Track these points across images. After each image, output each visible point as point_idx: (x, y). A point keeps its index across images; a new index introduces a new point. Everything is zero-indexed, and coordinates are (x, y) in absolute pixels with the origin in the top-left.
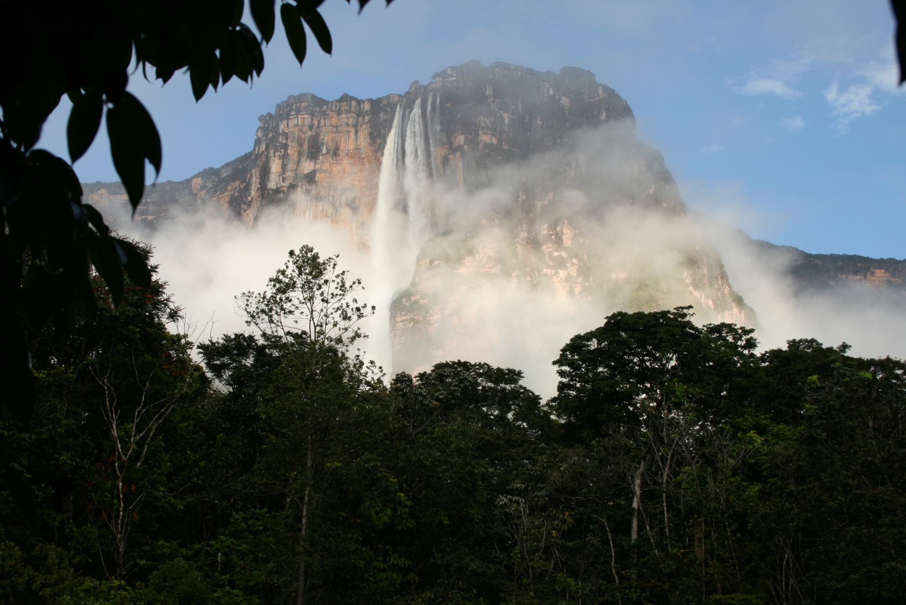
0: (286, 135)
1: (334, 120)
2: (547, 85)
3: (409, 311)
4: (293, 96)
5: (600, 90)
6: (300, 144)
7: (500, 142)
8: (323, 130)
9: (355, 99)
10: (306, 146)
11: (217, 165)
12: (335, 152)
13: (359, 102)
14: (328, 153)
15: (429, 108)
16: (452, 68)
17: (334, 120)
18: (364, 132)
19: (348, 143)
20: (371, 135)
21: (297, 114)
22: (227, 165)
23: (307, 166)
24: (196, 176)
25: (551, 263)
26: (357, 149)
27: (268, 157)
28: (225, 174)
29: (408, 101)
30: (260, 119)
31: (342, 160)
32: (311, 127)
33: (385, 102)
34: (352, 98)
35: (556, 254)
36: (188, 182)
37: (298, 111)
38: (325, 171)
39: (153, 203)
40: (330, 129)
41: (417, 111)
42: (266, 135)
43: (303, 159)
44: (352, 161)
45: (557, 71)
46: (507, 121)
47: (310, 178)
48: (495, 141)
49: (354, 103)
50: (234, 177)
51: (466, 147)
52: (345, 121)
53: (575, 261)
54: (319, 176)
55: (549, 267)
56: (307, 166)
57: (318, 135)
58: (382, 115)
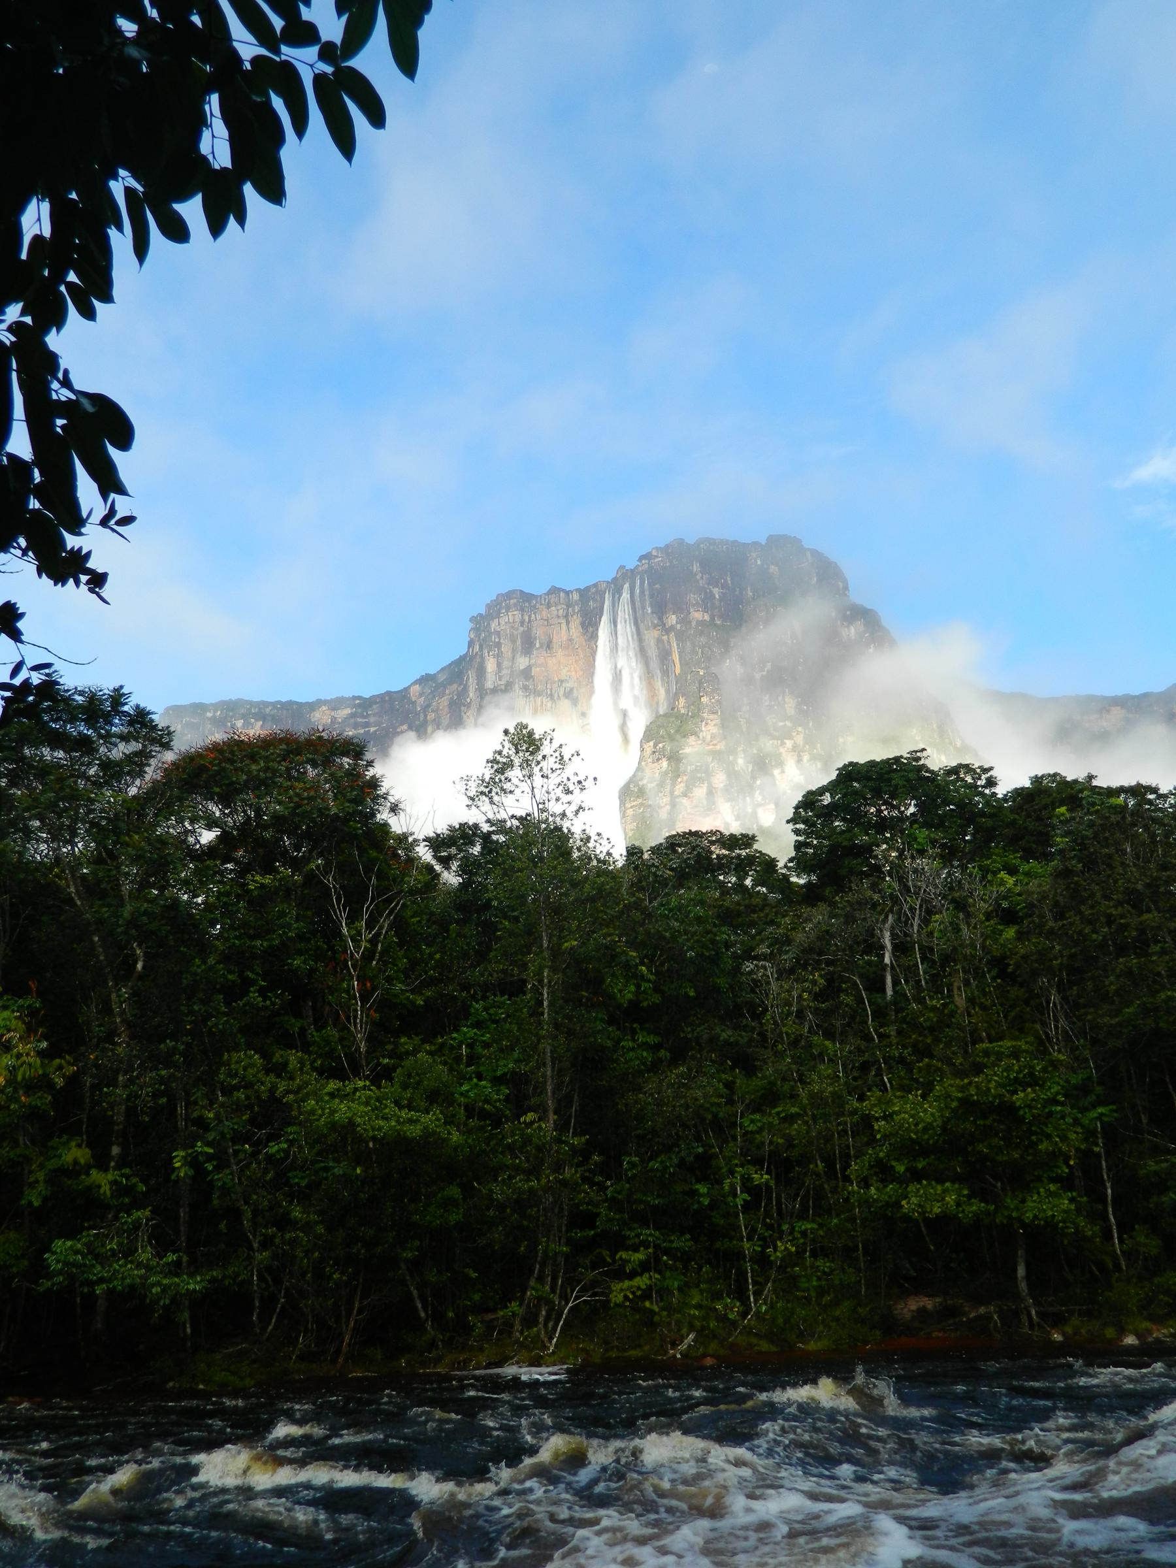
0: (498, 634)
1: (545, 614)
2: (754, 555)
4: (502, 595)
5: (808, 554)
6: (514, 641)
7: (712, 618)
8: (535, 624)
9: (563, 590)
10: (519, 642)
11: (432, 671)
12: (549, 646)
13: (567, 593)
14: (541, 646)
15: (637, 591)
16: (657, 548)
17: (545, 614)
18: (576, 622)
19: (561, 635)
20: (583, 624)
21: (507, 612)
22: (443, 669)
24: (415, 683)
25: (776, 734)
26: (571, 640)
27: (482, 657)
28: (442, 678)
29: (615, 587)
30: (472, 619)
32: (522, 623)
33: (593, 590)
34: (560, 590)
35: (781, 724)
36: (406, 689)
37: (508, 609)
39: (374, 715)
41: (626, 595)
42: (478, 636)
43: (518, 656)
45: (763, 542)
47: (527, 673)
48: (707, 617)
49: (562, 594)
50: (450, 681)
51: (678, 626)
53: (800, 729)
54: (535, 671)
56: (522, 662)
57: (529, 630)
58: (591, 603)
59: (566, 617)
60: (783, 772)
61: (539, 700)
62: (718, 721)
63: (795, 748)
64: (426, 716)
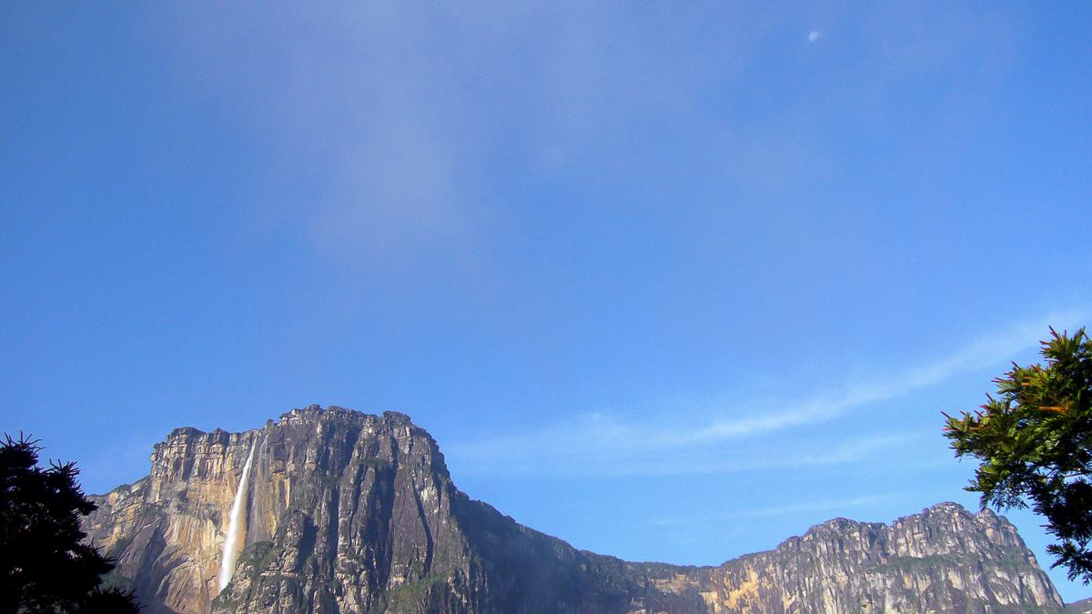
0: (168, 460)
3: (223, 607)
5: (407, 429)
6: (177, 466)
13: (228, 435)
22: (137, 482)
23: (181, 486)
28: (135, 489)
31: (210, 480)
35: (347, 561)
37: (180, 440)
38: (195, 490)
40: (203, 455)
44: (218, 482)
45: (380, 415)
46: (332, 453)
47: (183, 496)
50: (139, 493)
52: (216, 450)
55: (342, 572)
59: (223, 453)
60: (342, 600)
61: (187, 517)
62: (297, 553)
63: (357, 583)
64: (116, 519)
